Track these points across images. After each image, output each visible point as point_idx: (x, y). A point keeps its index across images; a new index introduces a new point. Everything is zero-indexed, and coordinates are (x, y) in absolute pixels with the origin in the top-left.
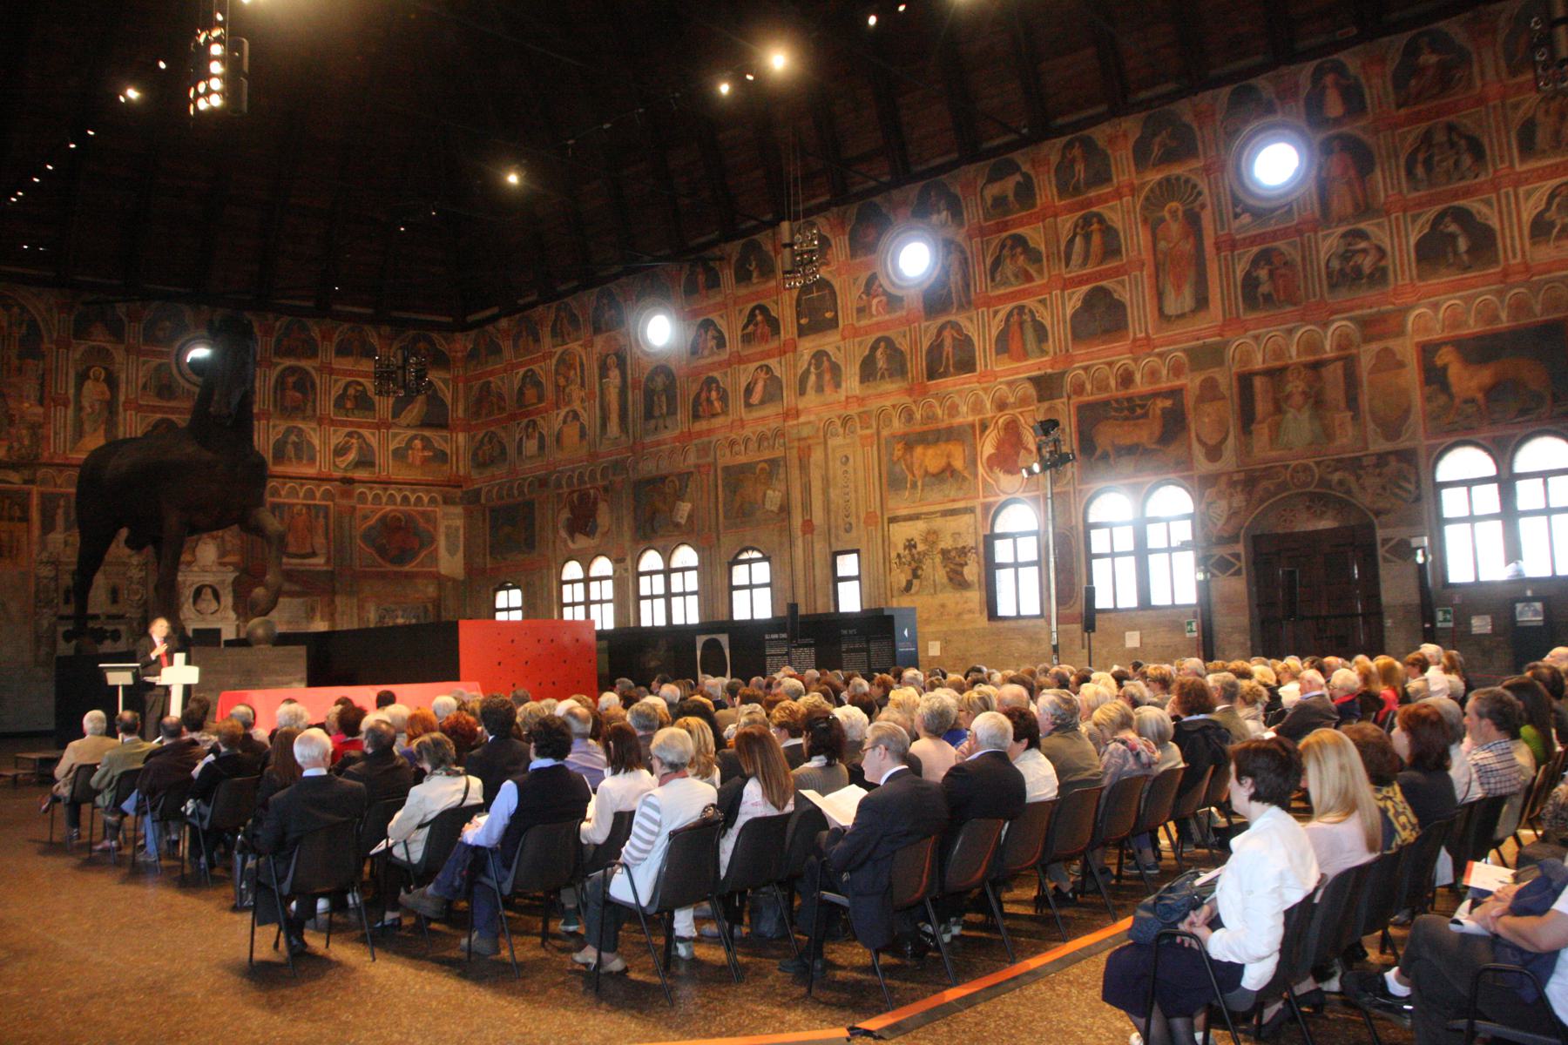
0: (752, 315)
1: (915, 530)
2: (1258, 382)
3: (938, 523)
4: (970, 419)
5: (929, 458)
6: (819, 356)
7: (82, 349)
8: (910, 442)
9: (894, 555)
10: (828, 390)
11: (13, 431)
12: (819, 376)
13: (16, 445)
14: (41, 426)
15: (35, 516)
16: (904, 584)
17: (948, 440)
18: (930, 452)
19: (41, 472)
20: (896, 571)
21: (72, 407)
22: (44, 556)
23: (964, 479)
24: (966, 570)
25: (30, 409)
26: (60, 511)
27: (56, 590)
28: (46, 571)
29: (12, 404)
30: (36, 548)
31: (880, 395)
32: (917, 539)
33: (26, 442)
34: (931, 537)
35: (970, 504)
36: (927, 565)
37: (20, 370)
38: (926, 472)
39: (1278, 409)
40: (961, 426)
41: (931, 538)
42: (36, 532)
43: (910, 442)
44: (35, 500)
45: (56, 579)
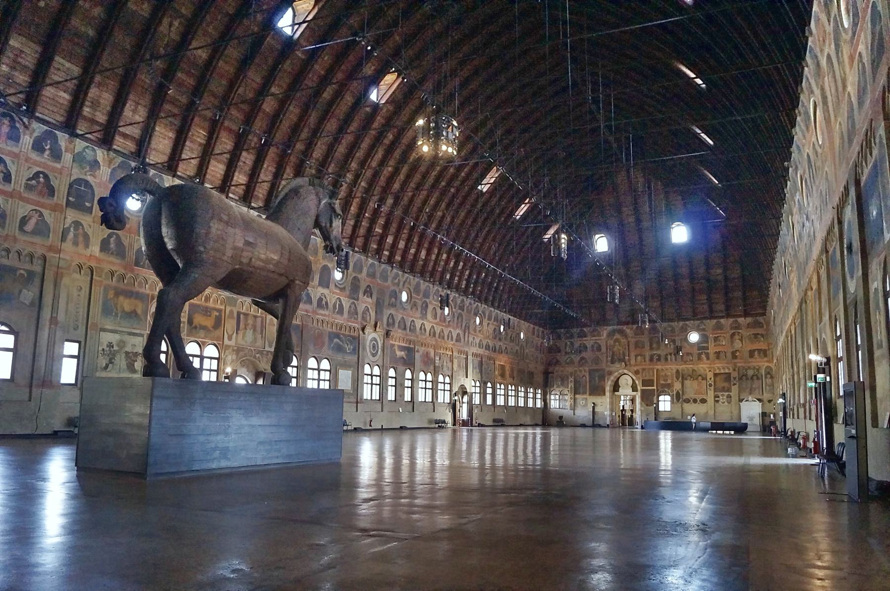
0: (37, 175)
1: (114, 338)
2: (242, 316)
3: (126, 338)
4: (148, 292)
5: (127, 304)
6: (77, 224)
8: (118, 293)
9: (100, 348)
10: (81, 246)
12: (75, 236)
16: (104, 365)
17: (136, 298)
18: (127, 301)
20: (101, 357)
23: (141, 320)
24: (136, 364)
31: (110, 262)
32: (114, 343)
34: (122, 344)
35: (142, 332)
36: (117, 358)
38: (123, 311)
39: (246, 329)
40: (142, 294)
41: (122, 344)
43: (118, 293)
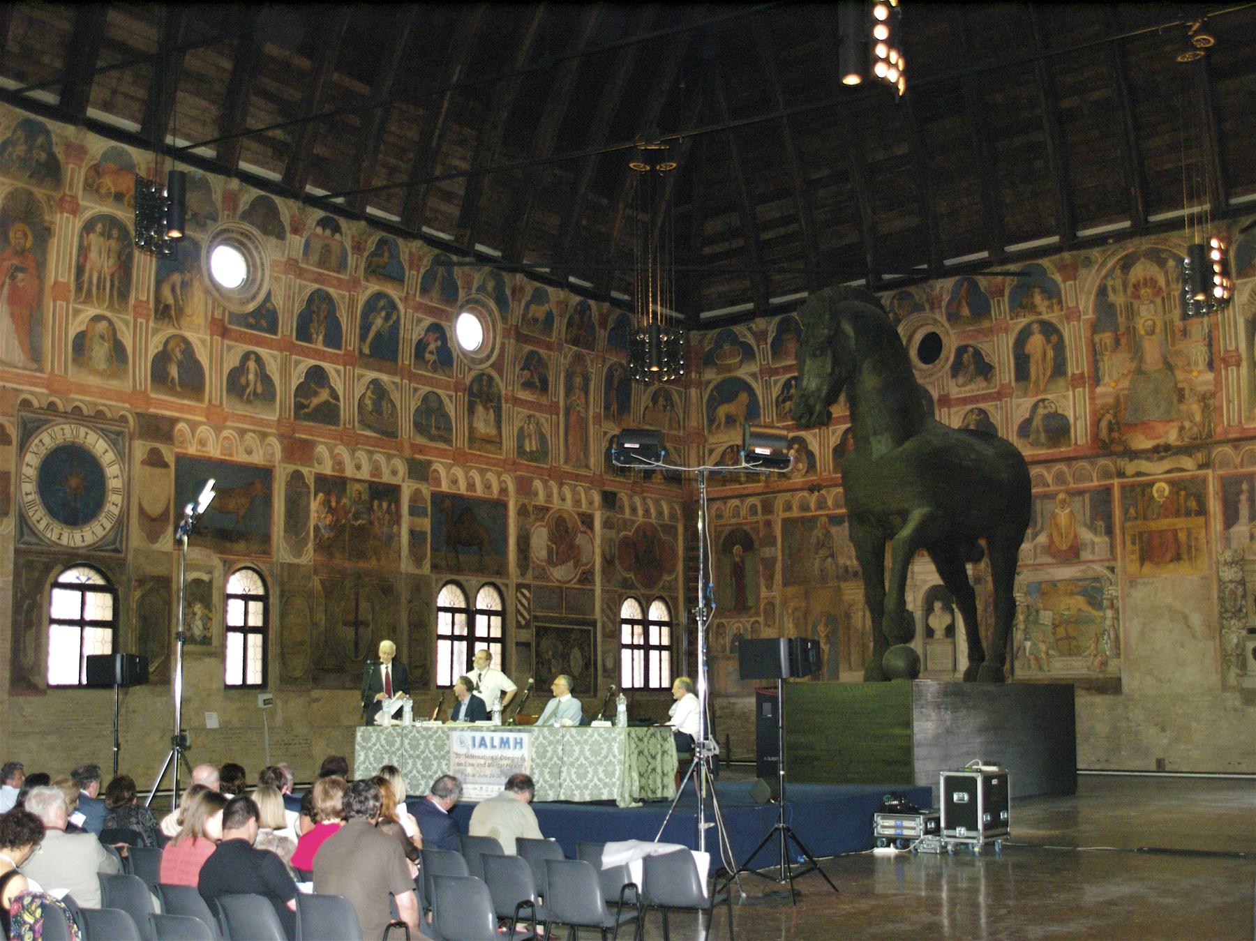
7: (1249, 287)
11: (1183, 407)
13: (1187, 424)
14: (1213, 395)
15: (1214, 506)
19: (1217, 451)
21: (1244, 365)
22: (1228, 555)
25: (1203, 379)
26: (1243, 497)
27: (1244, 596)
28: (1229, 574)
29: (1180, 375)
30: (1217, 546)
33: (1198, 418)
37: (1185, 333)
42: (1217, 524)
44: (1212, 488)
45: (1242, 582)
